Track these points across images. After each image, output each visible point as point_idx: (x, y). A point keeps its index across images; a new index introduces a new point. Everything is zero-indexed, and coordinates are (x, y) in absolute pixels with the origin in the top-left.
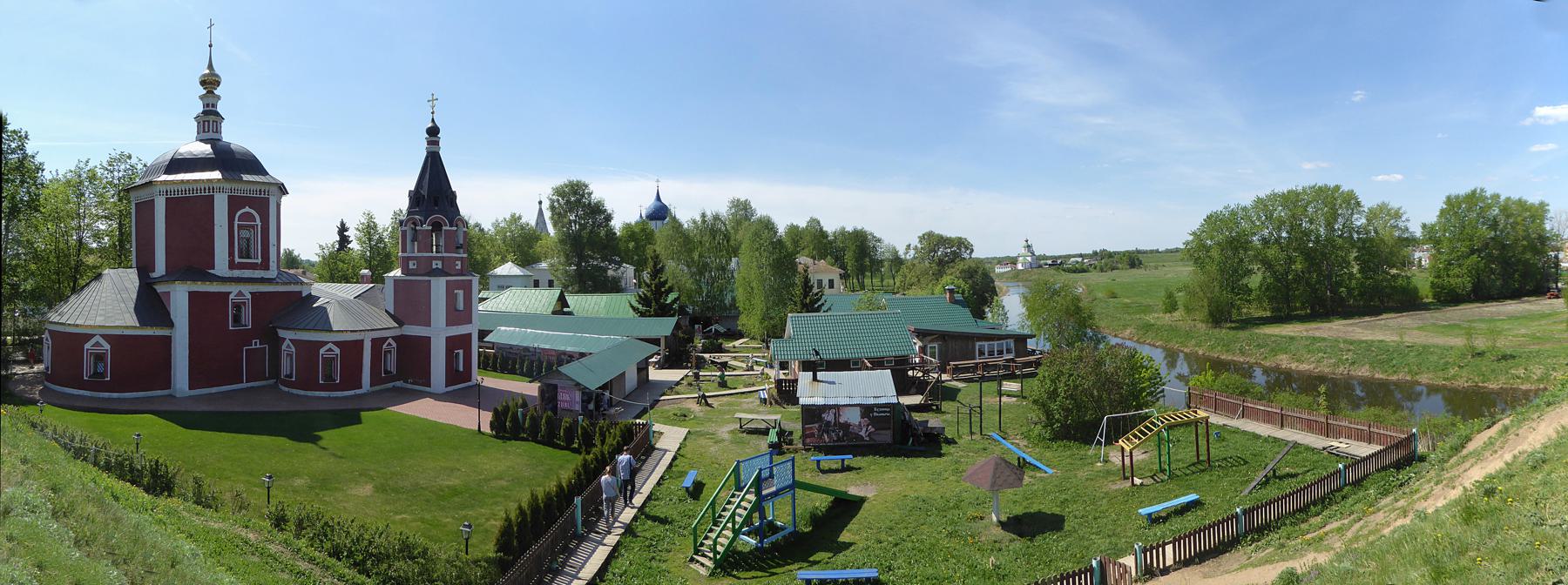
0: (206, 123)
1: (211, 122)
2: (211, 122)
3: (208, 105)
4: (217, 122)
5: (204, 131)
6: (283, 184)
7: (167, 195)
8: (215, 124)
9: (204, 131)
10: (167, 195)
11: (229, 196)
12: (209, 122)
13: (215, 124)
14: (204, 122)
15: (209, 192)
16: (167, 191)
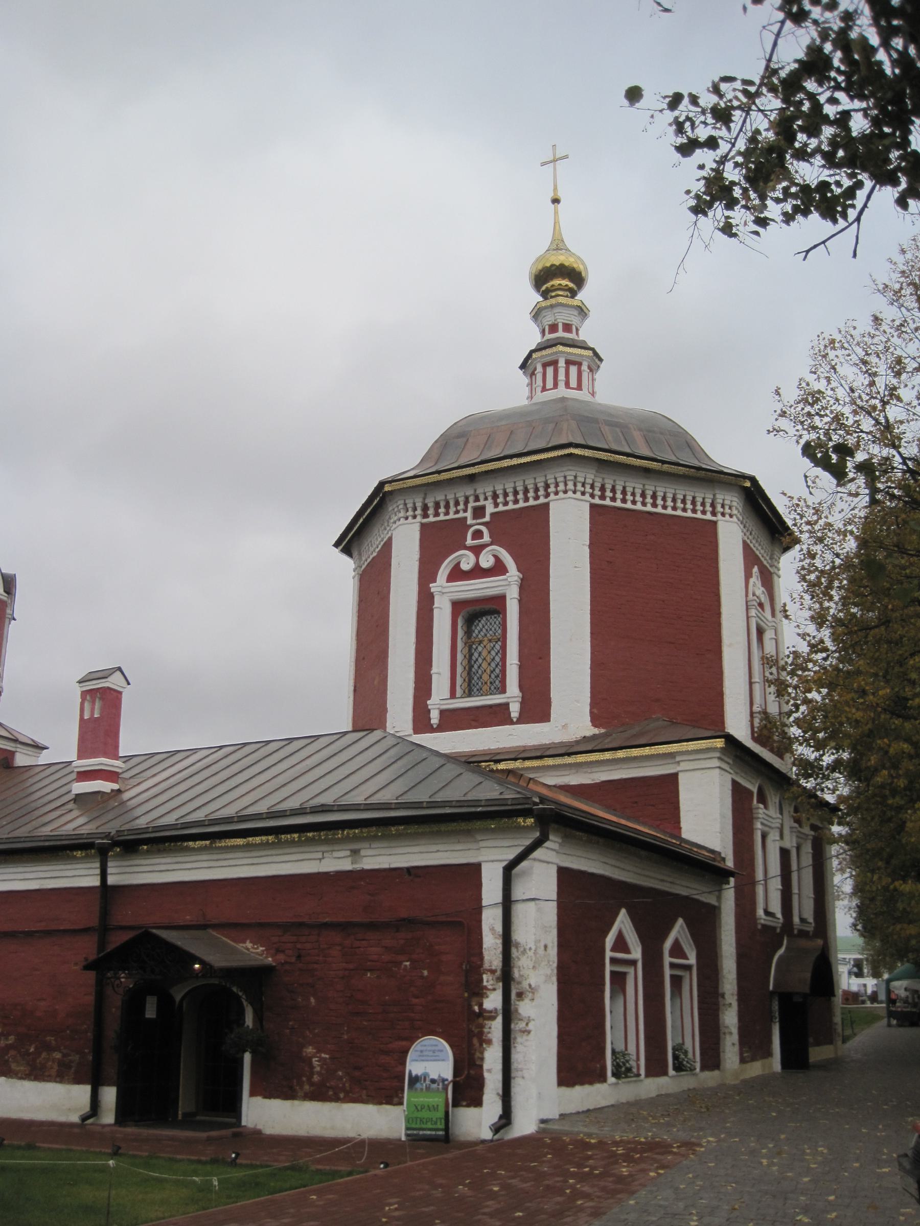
0: (550, 370)
1: (562, 363)
2: (562, 363)
3: (553, 328)
4: (579, 364)
5: (544, 389)
6: (753, 480)
7: (425, 516)
8: (573, 370)
9: (544, 389)
10: (425, 516)
11: (593, 506)
12: (555, 363)
13: (573, 370)
14: (545, 366)
15: (537, 498)
16: (425, 508)
